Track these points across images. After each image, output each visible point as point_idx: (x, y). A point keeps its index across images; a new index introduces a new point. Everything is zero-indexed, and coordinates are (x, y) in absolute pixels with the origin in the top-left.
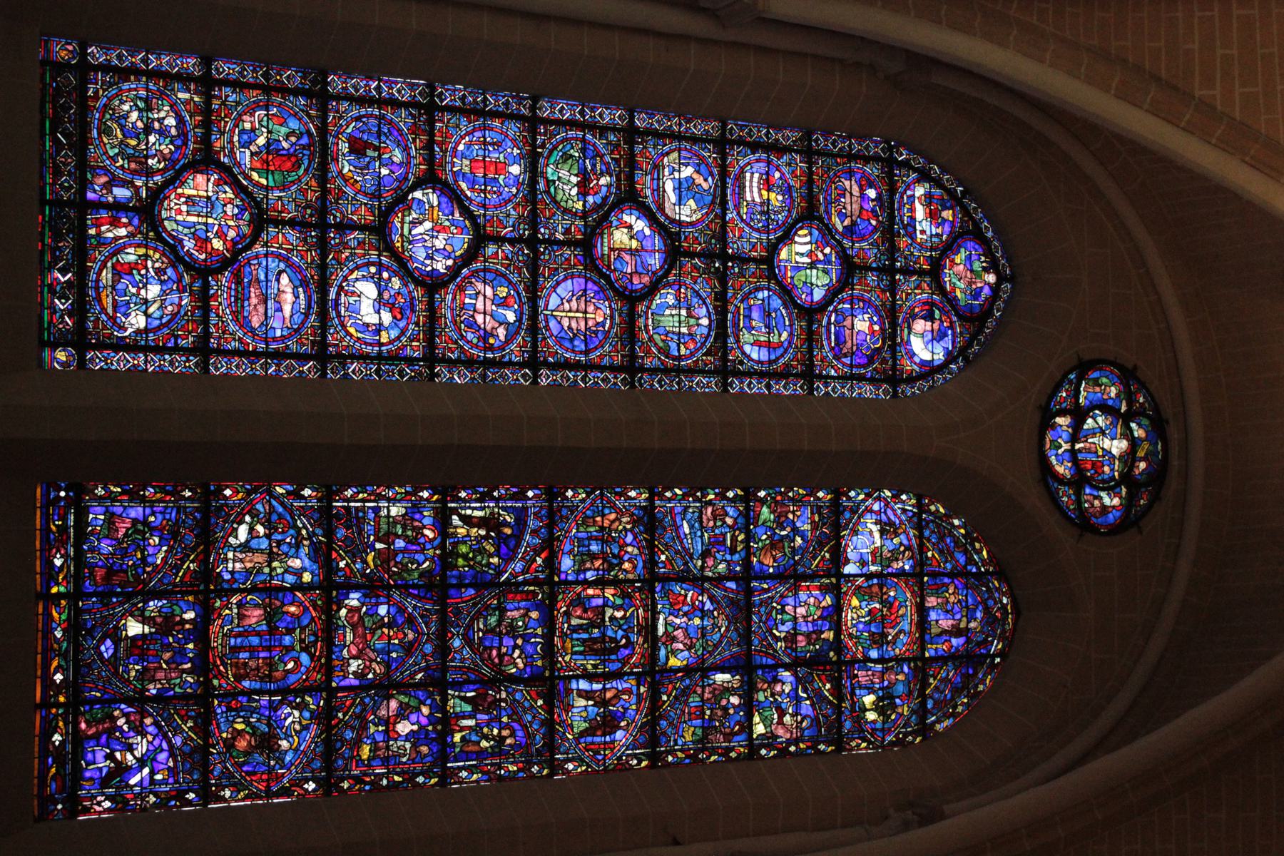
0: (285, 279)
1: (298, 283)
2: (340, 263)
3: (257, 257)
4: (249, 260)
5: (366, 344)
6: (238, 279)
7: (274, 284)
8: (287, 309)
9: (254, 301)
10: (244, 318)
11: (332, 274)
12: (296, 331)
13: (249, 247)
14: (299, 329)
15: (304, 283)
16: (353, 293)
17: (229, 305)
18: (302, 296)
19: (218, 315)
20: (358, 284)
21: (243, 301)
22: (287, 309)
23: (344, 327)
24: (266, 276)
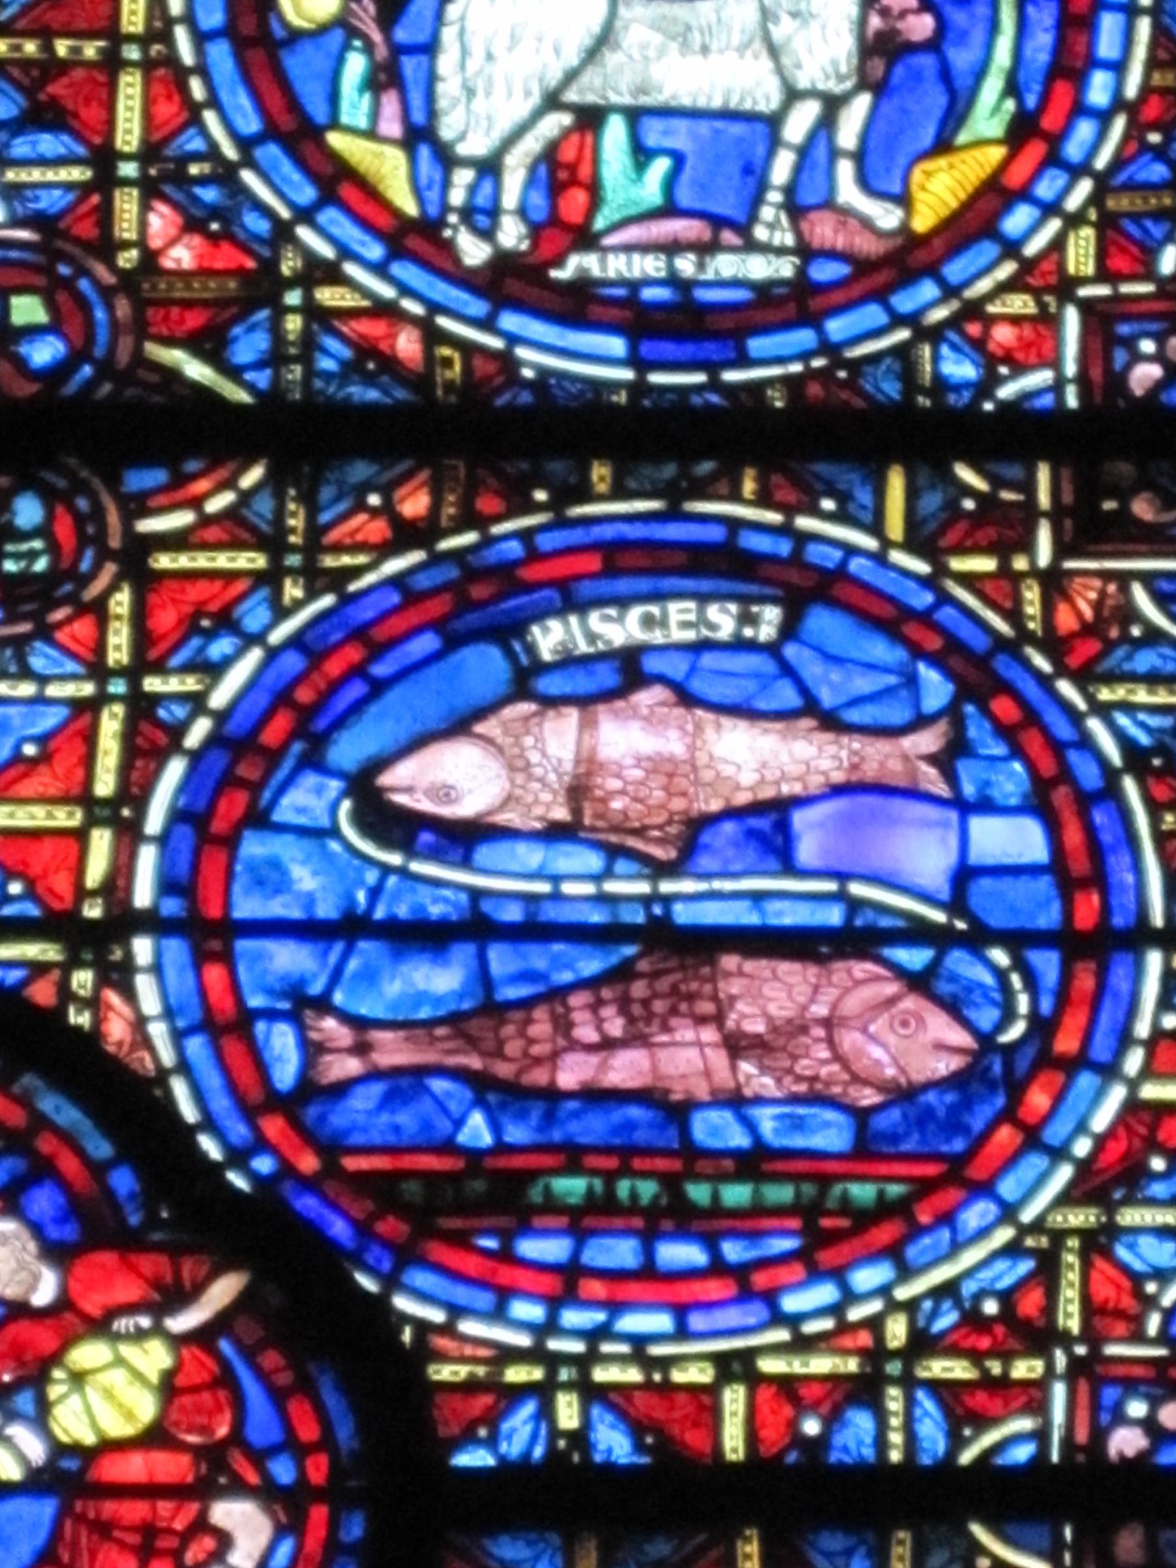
0: (457, 777)
1: (484, 666)
2: (261, 289)
3: (228, 1028)
4: (258, 1099)
5: (1070, 65)
6: (461, 1206)
7: (506, 876)
8: (749, 757)
9: (686, 1058)
10: (867, 1149)
11: (371, 359)
12: (980, 676)
13: (126, 1099)
14: (951, 655)
15: (483, 607)
16: (565, 173)
17: (749, 1285)
18: (617, 629)
19: (864, 1390)
20: (469, 127)
21: (695, 1159)
22: (749, 757)
23: (910, 258)
24: (423, 936)
